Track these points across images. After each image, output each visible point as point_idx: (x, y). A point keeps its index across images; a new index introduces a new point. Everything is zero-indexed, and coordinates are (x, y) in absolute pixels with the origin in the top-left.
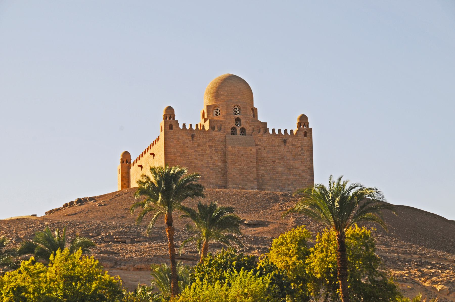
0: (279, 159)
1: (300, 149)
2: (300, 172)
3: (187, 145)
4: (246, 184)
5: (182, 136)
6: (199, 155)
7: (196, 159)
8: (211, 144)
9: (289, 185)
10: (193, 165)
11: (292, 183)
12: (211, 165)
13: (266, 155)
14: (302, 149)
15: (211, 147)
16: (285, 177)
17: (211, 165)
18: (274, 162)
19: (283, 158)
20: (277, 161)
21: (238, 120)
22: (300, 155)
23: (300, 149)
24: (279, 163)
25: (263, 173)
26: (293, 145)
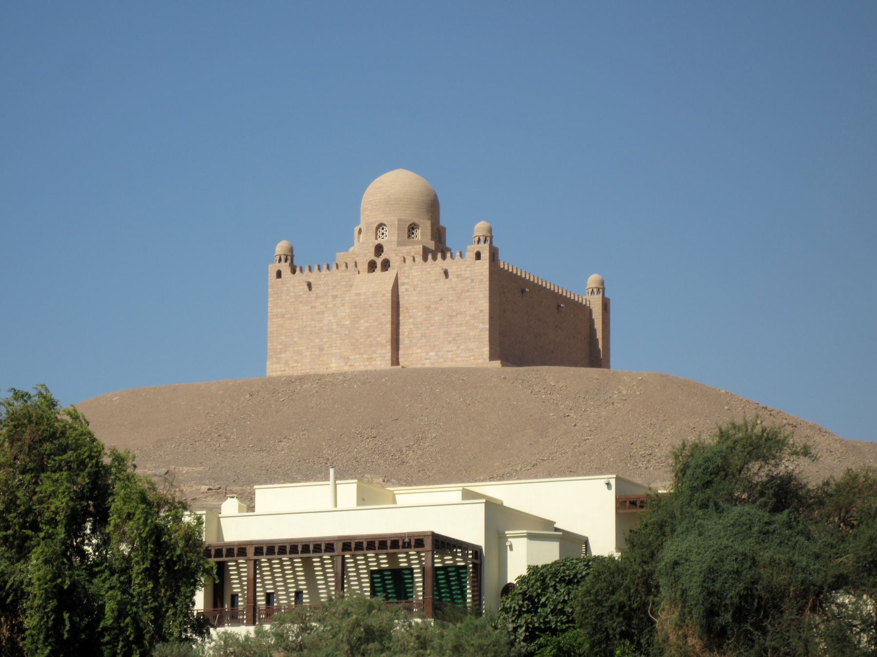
0: (436, 303)
1: (468, 281)
2: (468, 318)
3: (300, 300)
4: (374, 352)
5: (294, 286)
6: (318, 313)
7: (313, 320)
9: (450, 342)
11: (454, 339)
12: (334, 327)
13: (416, 298)
14: (472, 281)
15: (335, 297)
16: (444, 330)
17: (334, 327)
19: (441, 299)
21: (379, 249)
22: (468, 291)
23: (468, 281)
24: (436, 309)
25: (411, 329)
26: (458, 276)
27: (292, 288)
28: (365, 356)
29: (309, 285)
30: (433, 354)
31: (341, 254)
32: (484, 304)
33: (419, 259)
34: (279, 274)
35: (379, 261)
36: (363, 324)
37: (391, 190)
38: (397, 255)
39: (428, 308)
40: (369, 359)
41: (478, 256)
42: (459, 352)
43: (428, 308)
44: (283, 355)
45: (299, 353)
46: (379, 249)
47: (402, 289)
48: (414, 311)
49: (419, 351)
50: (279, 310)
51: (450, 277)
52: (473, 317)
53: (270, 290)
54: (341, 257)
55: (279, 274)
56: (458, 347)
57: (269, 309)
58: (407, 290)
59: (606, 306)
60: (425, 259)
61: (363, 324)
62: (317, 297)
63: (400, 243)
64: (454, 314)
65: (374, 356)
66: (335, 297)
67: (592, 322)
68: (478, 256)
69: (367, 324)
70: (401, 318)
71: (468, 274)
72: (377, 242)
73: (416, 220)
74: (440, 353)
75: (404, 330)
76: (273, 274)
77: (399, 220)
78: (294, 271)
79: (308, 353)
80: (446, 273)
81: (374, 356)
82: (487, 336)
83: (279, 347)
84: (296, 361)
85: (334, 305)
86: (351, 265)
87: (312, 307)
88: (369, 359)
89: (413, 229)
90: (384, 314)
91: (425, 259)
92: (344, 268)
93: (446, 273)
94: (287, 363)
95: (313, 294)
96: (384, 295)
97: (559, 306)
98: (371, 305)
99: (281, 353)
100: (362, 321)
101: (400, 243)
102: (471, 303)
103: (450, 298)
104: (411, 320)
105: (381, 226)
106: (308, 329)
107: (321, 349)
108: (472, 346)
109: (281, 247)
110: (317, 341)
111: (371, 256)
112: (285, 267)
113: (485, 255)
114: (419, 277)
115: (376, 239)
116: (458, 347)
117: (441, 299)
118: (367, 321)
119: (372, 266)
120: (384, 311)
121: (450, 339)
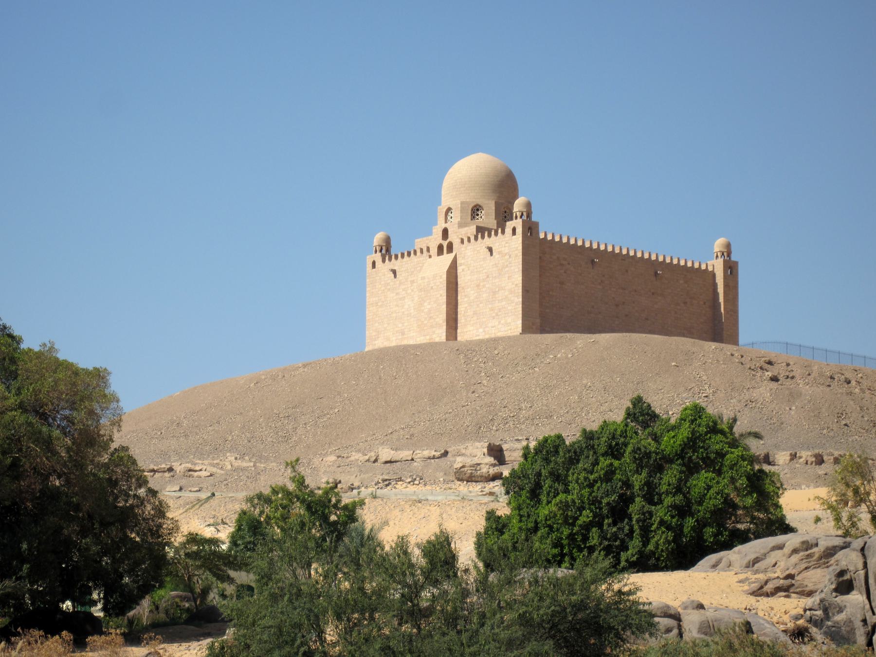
10: (394, 315)
11: (497, 315)
12: (412, 311)
15: (412, 282)
18: (478, 286)
19: (488, 277)
21: (445, 232)
24: (484, 286)
26: (499, 253)
29: (394, 272)
30: (481, 330)
31: (418, 240)
32: (518, 278)
33: (472, 238)
34: (374, 264)
35: (445, 244)
36: (427, 306)
37: (466, 173)
39: (478, 286)
41: (514, 230)
46: (445, 232)
47: (460, 269)
49: (472, 328)
51: (494, 254)
52: (511, 292)
54: (420, 243)
55: (374, 264)
58: (463, 270)
59: (731, 268)
60: (476, 238)
61: (427, 306)
62: (400, 283)
63: (461, 225)
66: (412, 282)
67: (715, 285)
68: (514, 230)
69: (429, 307)
70: (459, 298)
71: (506, 250)
72: (444, 225)
73: (479, 202)
75: (461, 308)
76: (370, 265)
77: (462, 203)
78: (384, 261)
80: (490, 250)
82: (520, 309)
83: (374, 334)
86: (425, 250)
87: (397, 294)
89: (478, 210)
91: (476, 238)
92: (418, 253)
93: (490, 250)
95: (397, 281)
96: (441, 277)
97: (656, 274)
100: (426, 304)
101: (461, 225)
102: (509, 278)
105: (449, 210)
106: (394, 315)
107: (403, 333)
108: (509, 320)
109: (378, 238)
110: (400, 325)
111: (440, 240)
112: (378, 257)
113: (519, 230)
114: (472, 257)
115: (446, 222)
116: (499, 322)
119: (440, 249)
120: (441, 292)
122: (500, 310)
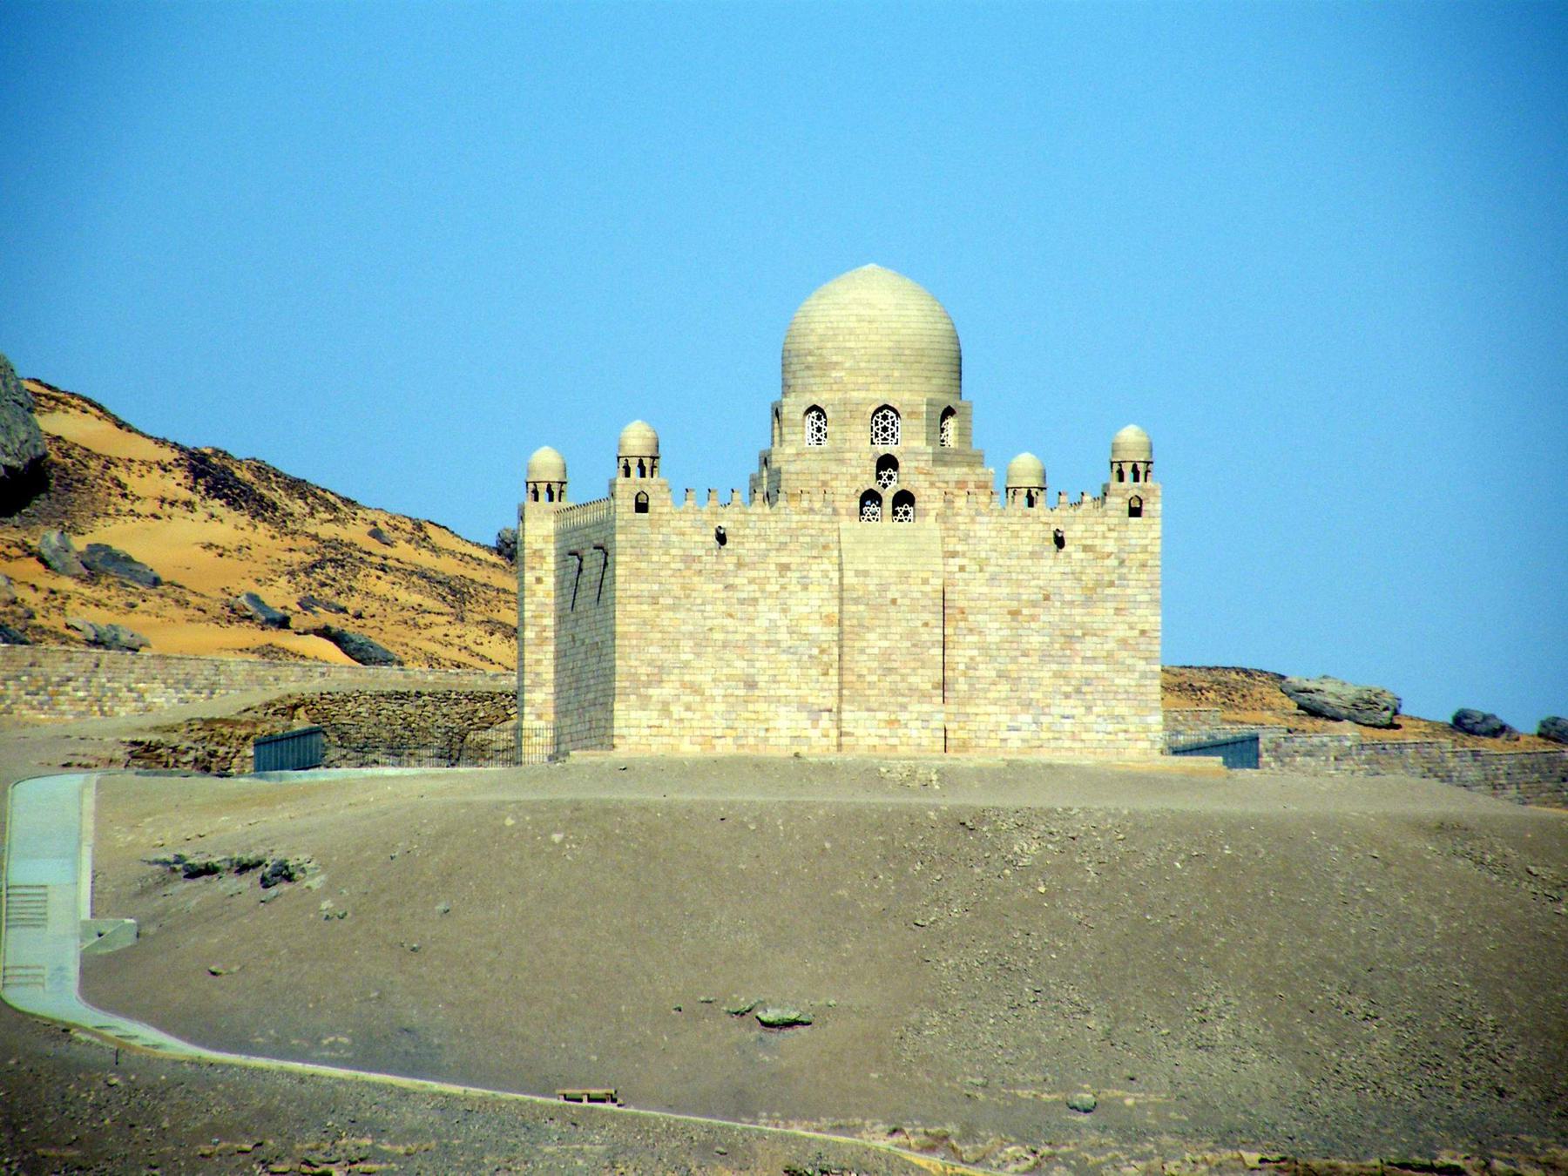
0: (1034, 604)
2: (1111, 645)
4: (904, 707)
6: (742, 602)
7: (731, 616)
8: (784, 560)
9: (1067, 696)
11: (1078, 691)
13: (985, 590)
14: (1122, 563)
15: (784, 568)
16: (1054, 667)
17: (783, 636)
19: (1047, 598)
20: (1025, 611)
22: (1111, 584)
24: (1033, 618)
26: (1086, 548)
27: (674, 538)
28: (882, 715)
29: (722, 539)
38: (932, 484)
39: (1015, 614)
40: (891, 723)
42: (1092, 718)
43: (1015, 614)
44: (651, 691)
45: (696, 689)
48: (980, 617)
50: (644, 586)
52: (1123, 643)
53: (618, 537)
56: (1089, 709)
57: (619, 580)
62: (740, 565)
64: (1079, 633)
65: (903, 716)
66: (784, 568)
71: (1111, 546)
72: (882, 450)
74: (1043, 719)
79: (715, 692)
81: (903, 716)
84: (688, 708)
85: (783, 587)
88: (891, 723)
90: (926, 625)
93: (1060, 542)
94: (665, 709)
98: (894, 601)
99: (649, 685)
100: (872, 636)
103: (1068, 598)
104: (975, 638)
107: (751, 685)
108: (1121, 709)
116: (1089, 709)
117: (1047, 598)
118: (884, 636)
120: (927, 617)
121: (1069, 689)
122: (1088, 681)
